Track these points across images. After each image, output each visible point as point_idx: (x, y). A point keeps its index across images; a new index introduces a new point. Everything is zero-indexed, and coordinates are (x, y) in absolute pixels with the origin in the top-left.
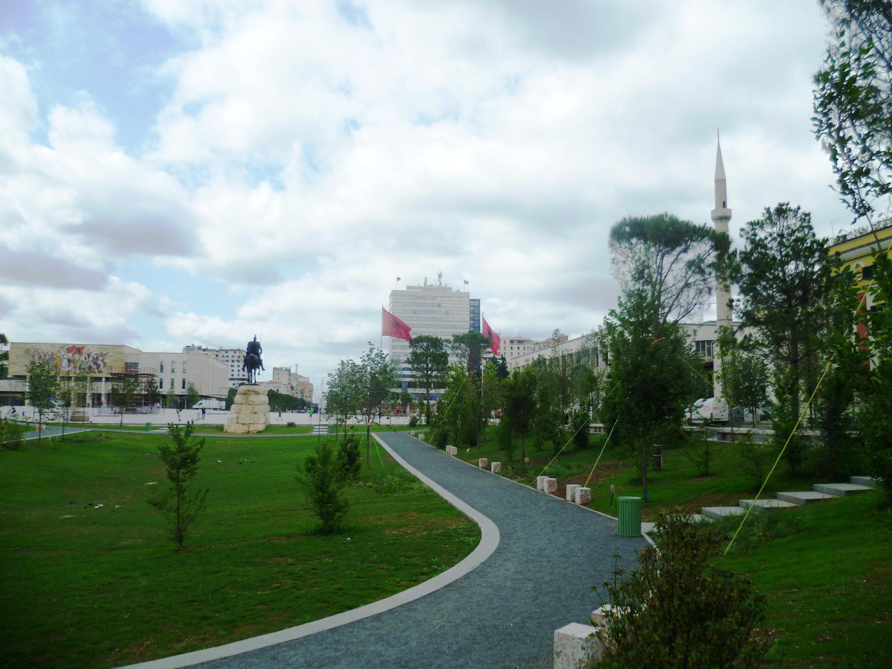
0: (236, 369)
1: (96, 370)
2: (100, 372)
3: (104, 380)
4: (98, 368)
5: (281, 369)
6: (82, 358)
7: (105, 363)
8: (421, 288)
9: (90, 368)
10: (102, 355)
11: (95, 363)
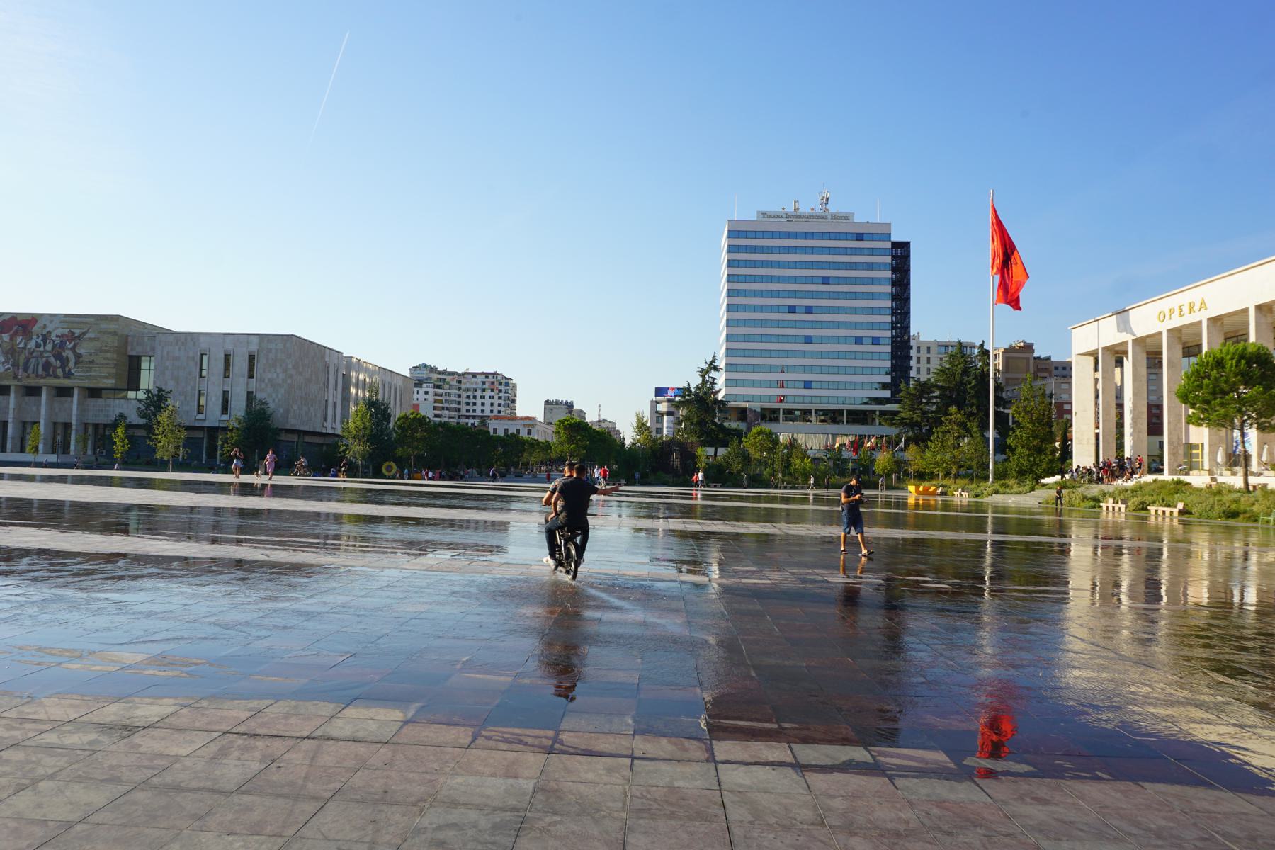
0: (488, 401)
1: (59, 372)
2: (68, 375)
3: (76, 392)
4: (63, 367)
5: (557, 403)
6: (32, 345)
7: (78, 356)
8: (787, 215)
9: (47, 366)
10: (72, 337)
11: (58, 356)
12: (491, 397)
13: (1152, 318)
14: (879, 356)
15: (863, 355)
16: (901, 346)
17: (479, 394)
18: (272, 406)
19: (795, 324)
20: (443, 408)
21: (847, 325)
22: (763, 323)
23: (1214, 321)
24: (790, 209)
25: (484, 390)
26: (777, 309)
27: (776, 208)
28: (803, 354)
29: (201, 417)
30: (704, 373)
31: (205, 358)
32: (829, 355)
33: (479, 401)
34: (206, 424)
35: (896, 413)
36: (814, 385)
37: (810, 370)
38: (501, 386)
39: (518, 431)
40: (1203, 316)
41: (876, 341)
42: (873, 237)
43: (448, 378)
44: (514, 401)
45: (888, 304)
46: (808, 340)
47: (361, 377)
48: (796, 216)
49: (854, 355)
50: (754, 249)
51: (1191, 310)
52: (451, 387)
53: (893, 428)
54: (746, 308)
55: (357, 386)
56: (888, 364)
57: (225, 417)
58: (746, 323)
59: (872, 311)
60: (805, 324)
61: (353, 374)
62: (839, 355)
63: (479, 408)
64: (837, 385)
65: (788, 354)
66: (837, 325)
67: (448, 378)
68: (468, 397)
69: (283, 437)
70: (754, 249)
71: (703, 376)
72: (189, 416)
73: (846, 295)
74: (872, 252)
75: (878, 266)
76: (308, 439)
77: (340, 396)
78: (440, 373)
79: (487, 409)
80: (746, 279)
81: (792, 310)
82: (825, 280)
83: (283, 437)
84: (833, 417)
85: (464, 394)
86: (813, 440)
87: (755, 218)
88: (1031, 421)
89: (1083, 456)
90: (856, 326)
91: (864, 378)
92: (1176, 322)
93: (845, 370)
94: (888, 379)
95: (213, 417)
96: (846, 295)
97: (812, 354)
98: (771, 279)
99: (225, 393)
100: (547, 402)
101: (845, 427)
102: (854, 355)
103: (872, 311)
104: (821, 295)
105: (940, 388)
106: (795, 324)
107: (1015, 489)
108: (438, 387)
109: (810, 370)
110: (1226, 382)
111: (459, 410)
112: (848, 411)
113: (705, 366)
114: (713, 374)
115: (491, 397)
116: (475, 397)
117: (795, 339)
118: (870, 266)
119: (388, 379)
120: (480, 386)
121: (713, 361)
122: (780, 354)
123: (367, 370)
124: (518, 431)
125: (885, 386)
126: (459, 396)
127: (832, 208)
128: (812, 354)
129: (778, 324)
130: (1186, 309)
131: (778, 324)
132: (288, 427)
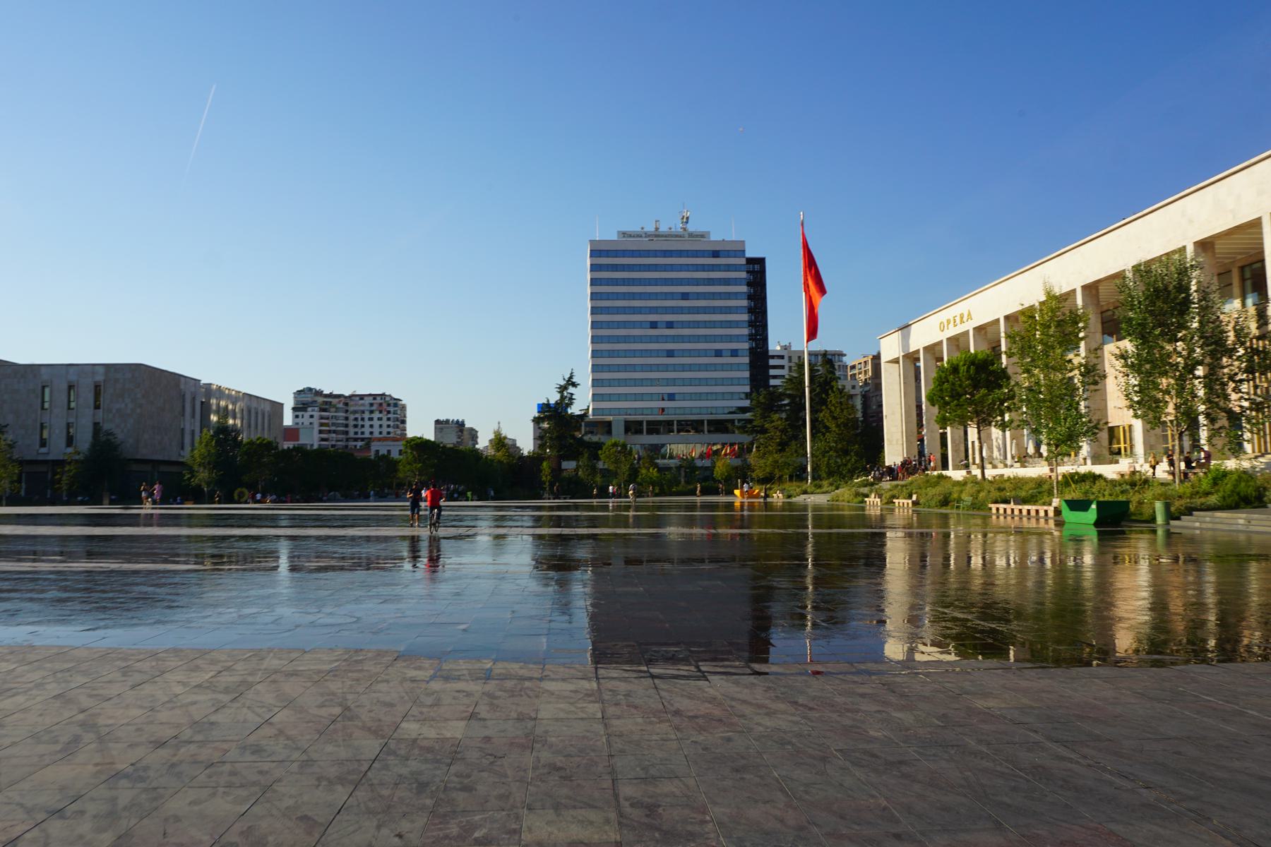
0: (376, 423)
5: (447, 421)
8: (647, 235)
12: (380, 419)
13: (928, 331)
14: (737, 367)
15: (723, 367)
16: (760, 356)
17: (367, 415)
18: (120, 436)
19: (657, 339)
20: (329, 432)
21: (707, 339)
22: (626, 339)
23: (979, 330)
24: (650, 228)
25: (372, 412)
26: (640, 325)
27: (634, 227)
28: (666, 368)
29: (43, 450)
30: (562, 389)
31: (47, 391)
32: (690, 368)
33: (367, 423)
34: (50, 458)
35: (750, 421)
36: (677, 397)
37: (673, 382)
38: (390, 408)
39: (389, 451)
40: (969, 326)
41: (734, 353)
42: (728, 254)
43: (334, 401)
44: (404, 422)
45: (745, 317)
46: (670, 354)
47: (223, 403)
48: (657, 235)
49: (715, 367)
50: (615, 268)
51: (962, 322)
52: (337, 410)
53: (745, 436)
54: (609, 325)
55: (217, 412)
56: (747, 374)
57: (70, 450)
58: (609, 339)
59: (730, 324)
60: (667, 339)
61: (213, 401)
62: (700, 368)
63: (367, 430)
64: (699, 397)
65: (650, 368)
66: (698, 339)
67: (334, 401)
68: (356, 419)
69: (134, 467)
70: (615, 268)
71: (561, 392)
72: (32, 451)
73: (705, 310)
74: (728, 268)
75: (735, 282)
76: (163, 468)
77: (198, 424)
78: (326, 396)
79: (376, 430)
80: (609, 296)
81: (654, 325)
82: (685, 296)
83: (134, 467)
84: (694, 426)
85: (352, 417)
86: (682, 448)
87: (615, 238)
88: (838, 426)
89: (894, 454)
90: (715, 338)
91: (727, 390)
92: (952, 331)
93: (706, 382)
94: (747, 389)
95: (57, 449)
96: (705, 310)
97: (675, 368)
98: (633, 296)
99: (68, 426)
100: (437, 422)
101: (707, 437)
102: (715, 367)
103: (730, 324)
104: (681, 310)
105: (789, 396)
106: (657, 339)
107: (825, 489)
108: (324, 410)
109: (673, 382)
110: (960, 386)
111: (347, 433)
112: (709, 421)
113: (563, 383)
114: (571, 390)
115: (380, 419)
116: (363, 419)
117: (657, 353)
118: (726, 282)
119: (254, 405)
120: (368, 408)
121: (571, 377)
122: (644, 368)
123: (229, 397)
124: (389, 451)
125: (748, 396)
126: (347, 419)
127: (691, 227)
128: (675, 368)
129: (640, 339)
130: (958, 320)
131: (640, 339)
132: (139, 457)
